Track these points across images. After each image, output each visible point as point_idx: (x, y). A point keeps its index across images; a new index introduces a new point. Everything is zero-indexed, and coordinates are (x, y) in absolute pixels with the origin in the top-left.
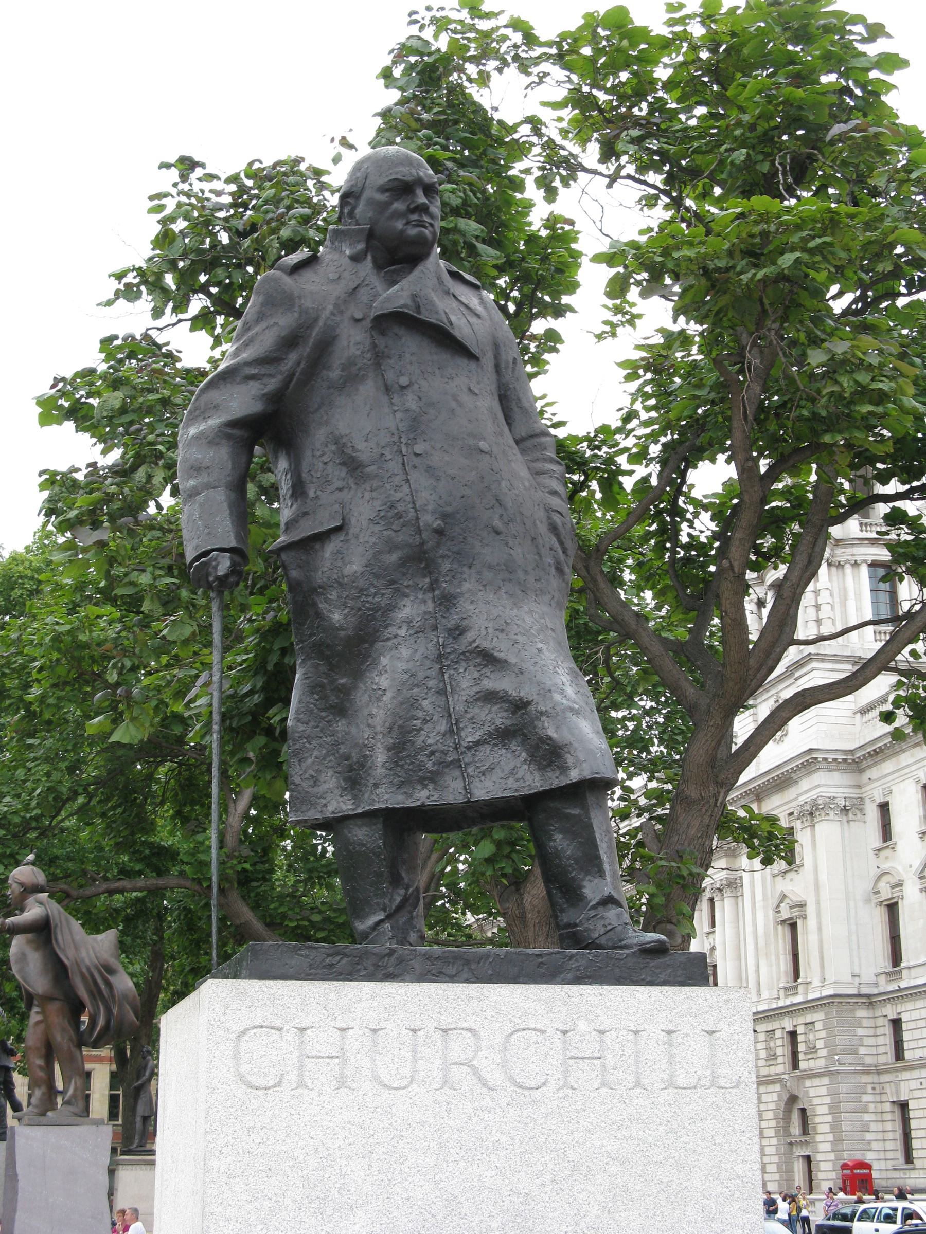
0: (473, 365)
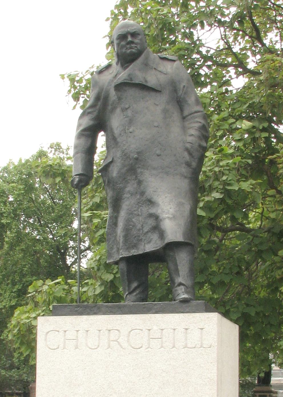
0: (158, 94)
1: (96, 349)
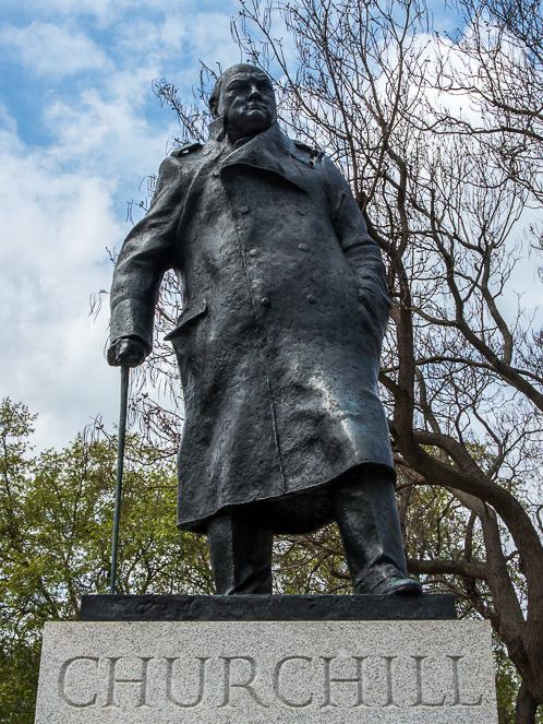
1: (194, 705)
